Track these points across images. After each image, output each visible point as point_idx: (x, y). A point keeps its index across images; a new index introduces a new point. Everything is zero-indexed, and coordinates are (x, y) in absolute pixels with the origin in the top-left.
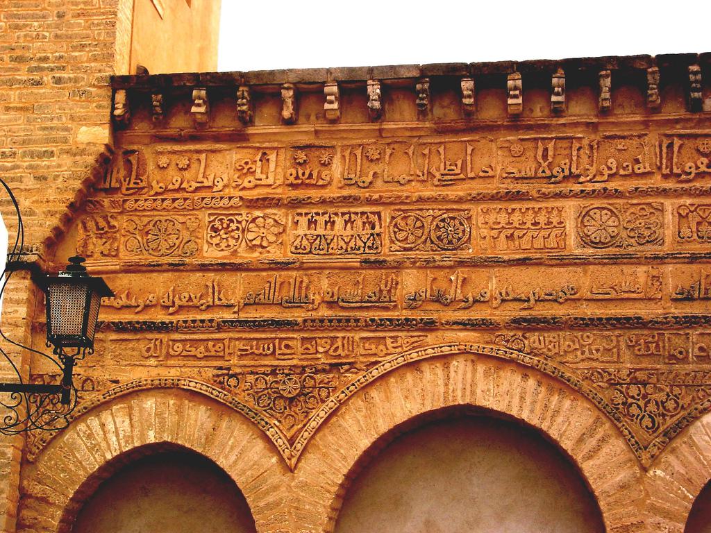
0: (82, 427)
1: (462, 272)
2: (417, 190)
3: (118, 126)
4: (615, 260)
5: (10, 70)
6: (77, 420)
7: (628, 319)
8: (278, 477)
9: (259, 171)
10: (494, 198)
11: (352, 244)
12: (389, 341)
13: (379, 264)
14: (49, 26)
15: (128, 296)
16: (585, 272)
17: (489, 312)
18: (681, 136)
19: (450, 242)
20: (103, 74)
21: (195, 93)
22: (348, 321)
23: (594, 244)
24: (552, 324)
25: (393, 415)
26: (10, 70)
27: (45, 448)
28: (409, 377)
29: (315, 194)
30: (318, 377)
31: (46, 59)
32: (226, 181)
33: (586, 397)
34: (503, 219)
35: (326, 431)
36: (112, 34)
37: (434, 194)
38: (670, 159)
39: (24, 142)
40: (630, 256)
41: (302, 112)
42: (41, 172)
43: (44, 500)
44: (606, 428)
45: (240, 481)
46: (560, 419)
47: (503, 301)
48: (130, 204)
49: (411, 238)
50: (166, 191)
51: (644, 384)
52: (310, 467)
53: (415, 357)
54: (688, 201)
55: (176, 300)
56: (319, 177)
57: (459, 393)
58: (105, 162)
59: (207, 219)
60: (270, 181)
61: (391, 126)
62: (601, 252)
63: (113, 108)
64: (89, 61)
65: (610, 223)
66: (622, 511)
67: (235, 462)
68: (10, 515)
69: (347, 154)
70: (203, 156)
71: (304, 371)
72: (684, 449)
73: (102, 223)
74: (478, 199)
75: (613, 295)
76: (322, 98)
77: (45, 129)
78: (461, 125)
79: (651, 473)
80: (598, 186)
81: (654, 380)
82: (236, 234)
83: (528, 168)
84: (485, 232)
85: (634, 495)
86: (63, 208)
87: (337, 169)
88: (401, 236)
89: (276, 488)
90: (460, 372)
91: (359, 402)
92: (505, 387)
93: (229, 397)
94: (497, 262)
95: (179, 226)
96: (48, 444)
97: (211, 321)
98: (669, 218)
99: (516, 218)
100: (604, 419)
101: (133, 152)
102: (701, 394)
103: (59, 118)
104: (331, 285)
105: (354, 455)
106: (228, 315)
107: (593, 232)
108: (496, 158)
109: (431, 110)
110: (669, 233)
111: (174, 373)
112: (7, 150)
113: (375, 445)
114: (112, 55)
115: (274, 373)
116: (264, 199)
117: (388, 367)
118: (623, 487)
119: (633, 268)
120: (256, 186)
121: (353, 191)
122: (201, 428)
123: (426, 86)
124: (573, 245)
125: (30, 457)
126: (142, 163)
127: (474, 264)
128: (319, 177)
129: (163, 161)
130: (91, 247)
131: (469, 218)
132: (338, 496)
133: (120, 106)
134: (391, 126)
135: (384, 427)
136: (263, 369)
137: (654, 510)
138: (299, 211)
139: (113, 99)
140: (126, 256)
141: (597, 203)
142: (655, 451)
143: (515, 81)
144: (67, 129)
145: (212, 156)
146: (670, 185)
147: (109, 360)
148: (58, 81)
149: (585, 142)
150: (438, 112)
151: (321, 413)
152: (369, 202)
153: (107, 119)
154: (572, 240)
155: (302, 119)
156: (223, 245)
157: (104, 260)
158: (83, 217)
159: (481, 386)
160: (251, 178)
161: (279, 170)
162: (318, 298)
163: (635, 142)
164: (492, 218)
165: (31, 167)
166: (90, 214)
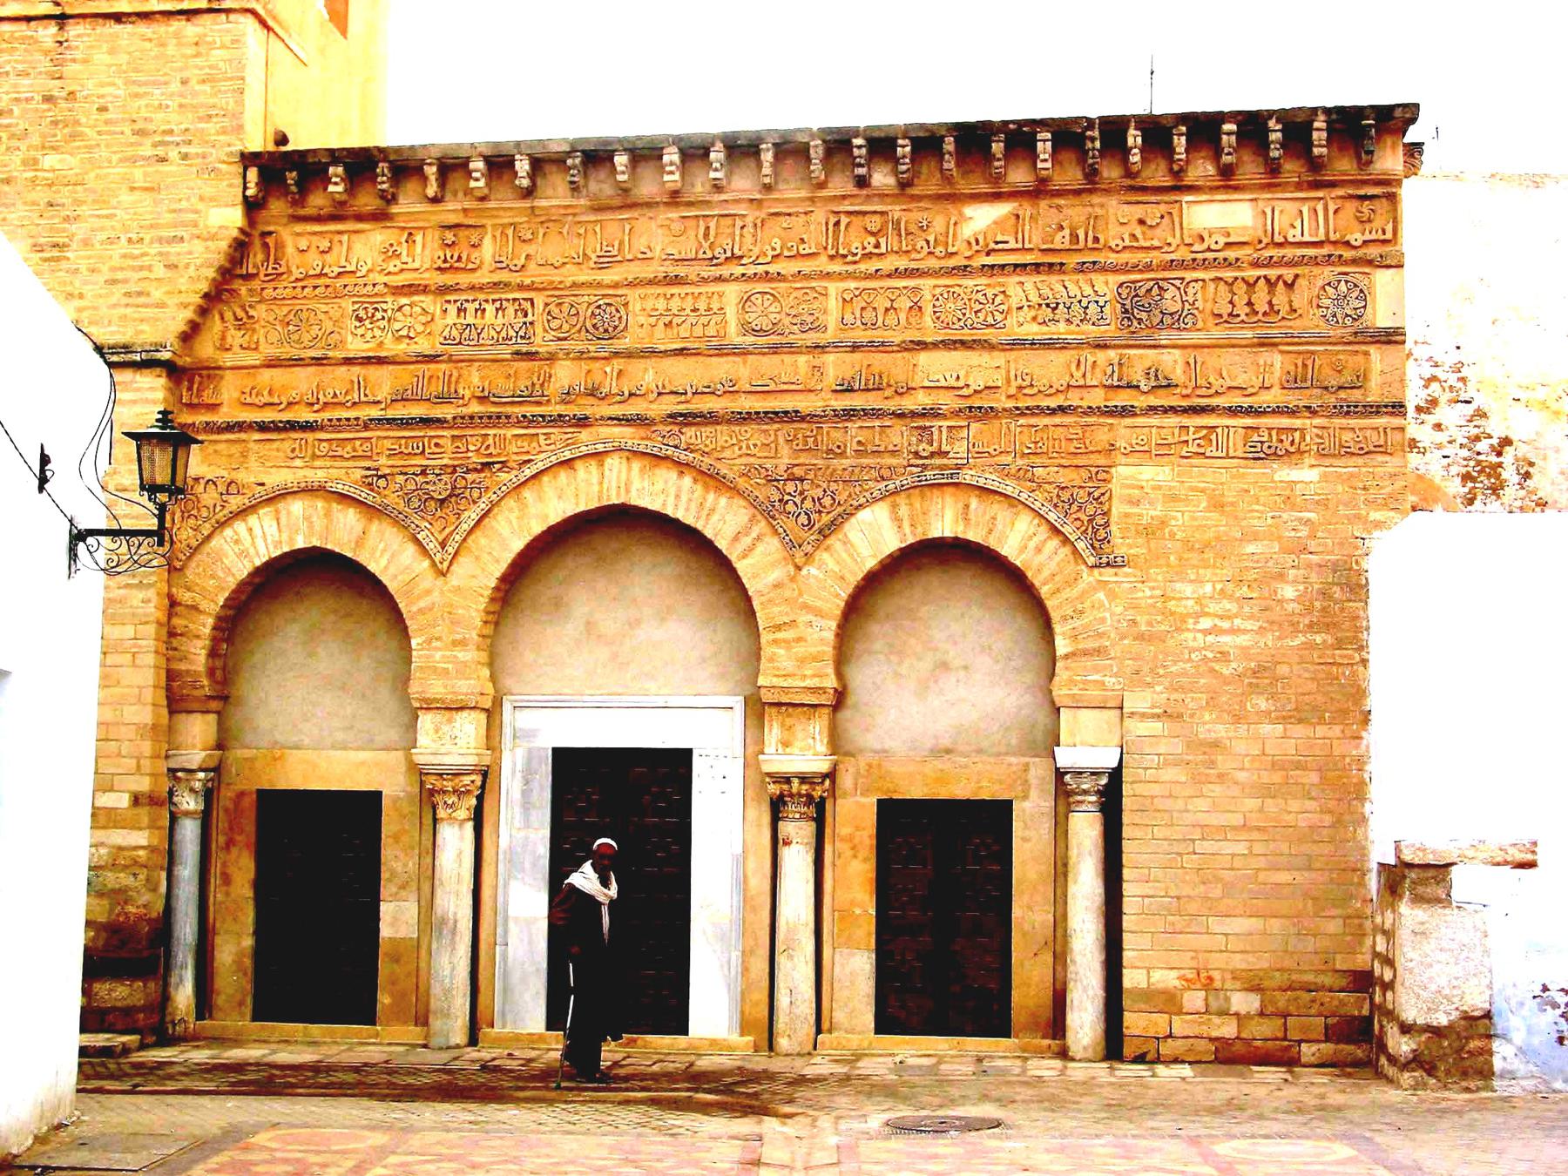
0: (228, 532)
1: (618, 364)
2: (572, 275)
3: (252, 207)
4: (775, 349)
5: (132, 144)
6: (222, 525)
7: (786, 413)
8: (428, 580)
9: (404, 253)
10: (651, 282)
11: (503, 334)
12: (542, 438)
13: (531, 356)
14: (172, 94)
15: (270, 393)
16: (745, 363)
17: (645, 405)
19: (606, 331)
20: (233, 149)
21: (331, 170)
22: (499, 417)
24: (710, 419)
25: (547, 516)
26: (132, 144)
27: (192, 555)
28: (563, 476)
29: (464, 279)
30: (470, 477)
31: (171, 132)
32: (369, 265)
33: (740, 494)
34: (661, 305)
35: (478, 533)
36: (240, 103)
37: (590, 278)
38: (836, 239)
39: (151, 226)
40: (791, 345)
41: (450, 187)
42: (173, 259)
43: (195, 608)
44: (761, 526)
45: (392, 587)
46: (715, 518)
47: (660, 394)
48: (269, 293)
49: (566, 327)
50: (307, 276)
51: (802, 480)
52: (463, 570)
53: (568, 455)
54: (852, 285)
55: (321, 396)
56: (468, 259)
57: (614, 492)
58: (240, 247)
59: (351, 308)
60: (416, 265)
61: (544, 203)
62: (762, 341)
63: (245, 188)
64: (218, 133)
65: (772, 309)
66: (776, 609)
67: (386, 568)
68: (159, 623)
69: (498, 234)
70: (345, 238)
71: (455, 471)
72: (838, 546)
73: (240, 314)
75: (772, 387)
76: (469, 174)
77: (174, 211)
78: (617, 202)
79: (804, 572)
80: (760, 269)
81: (811, 476)
82: (382, 324)
83: (688, 247)
84: (642, 320)
85: (788, 594)
86: (197, 299)
87: (488, 249)
88: (555, 324)
89: (428, 592)
90: (615, 471)
91: (510, 502)
92: (659, 486)
93: (378, 499)
94: (653, 353)
95: (322, 316)
97: (357, 419)
98: (833, 304)
99: (675, 304)
100: (759, 517)
101: (270, 233)
102: (858, 489)
103: (188, 199)
104: (482, 378)
105: (507, 557)
106: (375, 413)
108: (656, 237)
109: (586, 186)
110: (832, 321)
111: (320, 475)
112: (134, 237)
113: (529, 547)
114: (240, 128)
115: (423, 473)
116: (410, 286)
117: (541, 466)
118: (777, 586)
119: (794, 357)
120: (402, 270)
121: (504, 276)
122: (350, 533)
123: (578, 161)
124: (734, 336)
125: (178, 564)
126: (280, 246)
127: (629, 355)
128: (468, 259)
129: (303, 244)
130: (229, 340)
131: (626, 305)
132: (493, 600)
133: (251, 185)
134: (544, 203)
135: (538, 528)
136: (411, 470)
137: (806, 607)
138: (448, 298)
139: (245, 177)
140: (268, 350)
141: (760, 287)
142: (809, 549)
143: (671, 156)
144: (196, 212)
145: (354, 237)
146: (836, 267)
147: (253, 462)
148: (185, 157)
149: (749, 220)
150: (593, 186)
151: (472, 515)
152: (521, 287)
153: (240, 198)
154: (733, 328)
155: (448, 196)
156: (369, 334)
157: (243, 354)
158: (220, 306)
159: (637, 484)
160: (397, 262)
161: (427, 252)
162: (468, 394)
163: (802, 218)
164: (649, 305)
165: (160, 254)
166: (226, 303)
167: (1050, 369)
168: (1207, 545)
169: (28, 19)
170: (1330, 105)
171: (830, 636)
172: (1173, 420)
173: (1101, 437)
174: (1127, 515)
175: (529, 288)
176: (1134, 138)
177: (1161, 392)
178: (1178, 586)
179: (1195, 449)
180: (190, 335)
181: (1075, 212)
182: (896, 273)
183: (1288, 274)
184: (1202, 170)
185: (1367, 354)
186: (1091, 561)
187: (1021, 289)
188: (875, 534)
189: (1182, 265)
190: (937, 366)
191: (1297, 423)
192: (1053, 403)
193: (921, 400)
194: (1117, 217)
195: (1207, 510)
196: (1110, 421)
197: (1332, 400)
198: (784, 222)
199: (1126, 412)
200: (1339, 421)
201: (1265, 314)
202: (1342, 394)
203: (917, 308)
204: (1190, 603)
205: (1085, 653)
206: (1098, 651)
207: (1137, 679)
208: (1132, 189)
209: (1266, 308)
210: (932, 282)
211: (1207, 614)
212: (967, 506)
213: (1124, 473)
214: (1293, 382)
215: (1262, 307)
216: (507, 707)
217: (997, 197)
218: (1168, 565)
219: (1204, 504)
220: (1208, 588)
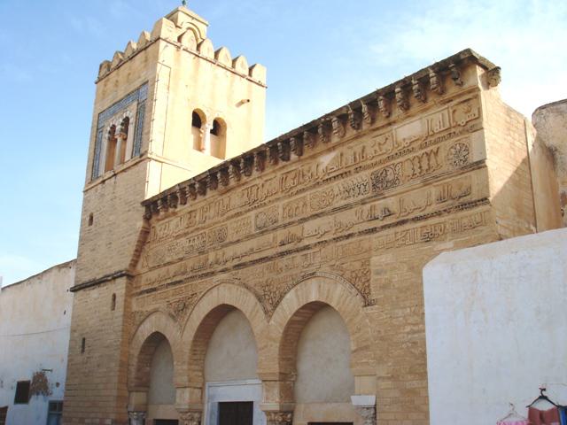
2: (216, 219)
3: (147, 219)
6: (139, 326)
10: (232, 217)
18: (288, 172)
23: (259, 228)
29: (191, 229)
54: (286, 201)
58: (146, 233)
74: (228, 218)
96: (134, 335)
98: (280, 210)
106: (169, 281)
107: (260, 223)
111: (157, 306)
124: (253, 232)
127: (227, 245)
135: (203, 316)
140: (151, 266)
154: (253, 228)
167: (347, 217)
168: (408, 289)
169: (110, 178)
170: (432, 63)
171: (277, 349)
172: (392, 231)
173: (366, 245)
174: (376, 280)
175: (203, 228)
176: (365, 108)
177: (388, 218)
178: (396, 311)
179: (402, 242)
180: (134, 264)
181: (357, 146)
182: (297, 193)
183: (434, 148)
184: (397, 112)
185: (470, 176)
186: (363, 304)
187: (337, 186)
188: (291, 303)
189: (393, 158)
190: (310, 226)
191: (442, 219)
192: (347, 233)
193: (306, 242)
194: (371, 144)
195: (408, 271)
196: (367, 236)
197: (457, 204)
198: (268, 183)
199: (373, 230)
200: (461, 214)
201: (427, 170)
202: (461, 200)
203: (305, 204)
204: (401, 319)
205: (361, 349)
206: (367, 348)
207: (380, 361)
208: (374, 130)
209: (427, 167)
210: (308, 193)
211: (409, 324)
212: (320, 286)
213: (377, 260)
214: (441, 199)
215: (425, 167)
216: (207, 385)
217: (329, 150)
218: (392, 302)
219: (406, 269)
220: (408, 310)
